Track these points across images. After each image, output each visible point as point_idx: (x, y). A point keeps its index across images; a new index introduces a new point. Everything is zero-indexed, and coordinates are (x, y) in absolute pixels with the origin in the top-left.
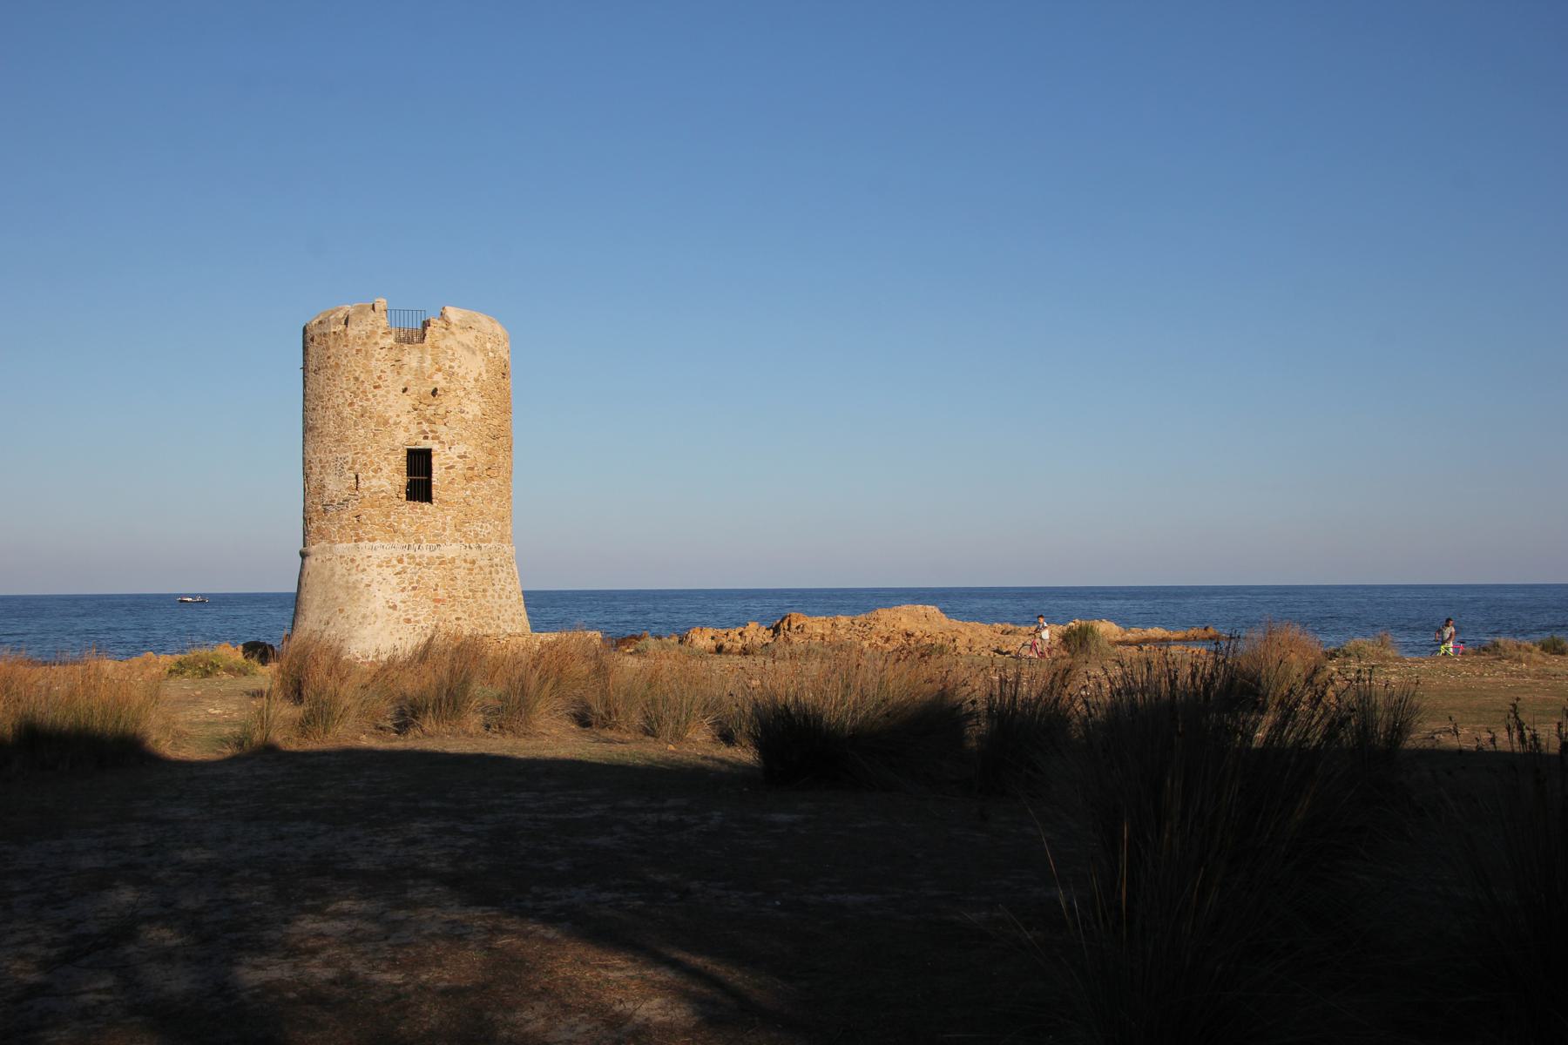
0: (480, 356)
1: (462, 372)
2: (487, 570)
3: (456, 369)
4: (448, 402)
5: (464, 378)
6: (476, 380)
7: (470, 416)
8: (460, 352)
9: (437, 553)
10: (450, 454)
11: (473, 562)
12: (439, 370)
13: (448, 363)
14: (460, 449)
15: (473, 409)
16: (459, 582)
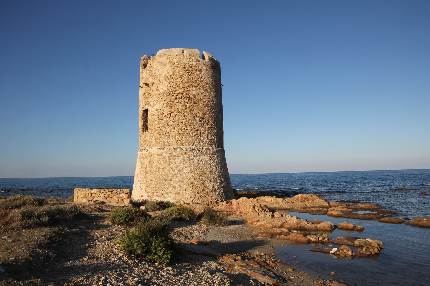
0: (168, 66)
1: (158, 74)
2: (168, 158)
3: (157, 74)
4: (153, 88)
5: (160, 76)
6: (165, 76)
7: (161, 92)
8: (158, 66)
9: (148, 152)
10: (153, 110)
11: (161, 155)
12: (151, 76)
13: (154, 72)
14: (157, 106)
15: (163, 88)
16: (154, 164)
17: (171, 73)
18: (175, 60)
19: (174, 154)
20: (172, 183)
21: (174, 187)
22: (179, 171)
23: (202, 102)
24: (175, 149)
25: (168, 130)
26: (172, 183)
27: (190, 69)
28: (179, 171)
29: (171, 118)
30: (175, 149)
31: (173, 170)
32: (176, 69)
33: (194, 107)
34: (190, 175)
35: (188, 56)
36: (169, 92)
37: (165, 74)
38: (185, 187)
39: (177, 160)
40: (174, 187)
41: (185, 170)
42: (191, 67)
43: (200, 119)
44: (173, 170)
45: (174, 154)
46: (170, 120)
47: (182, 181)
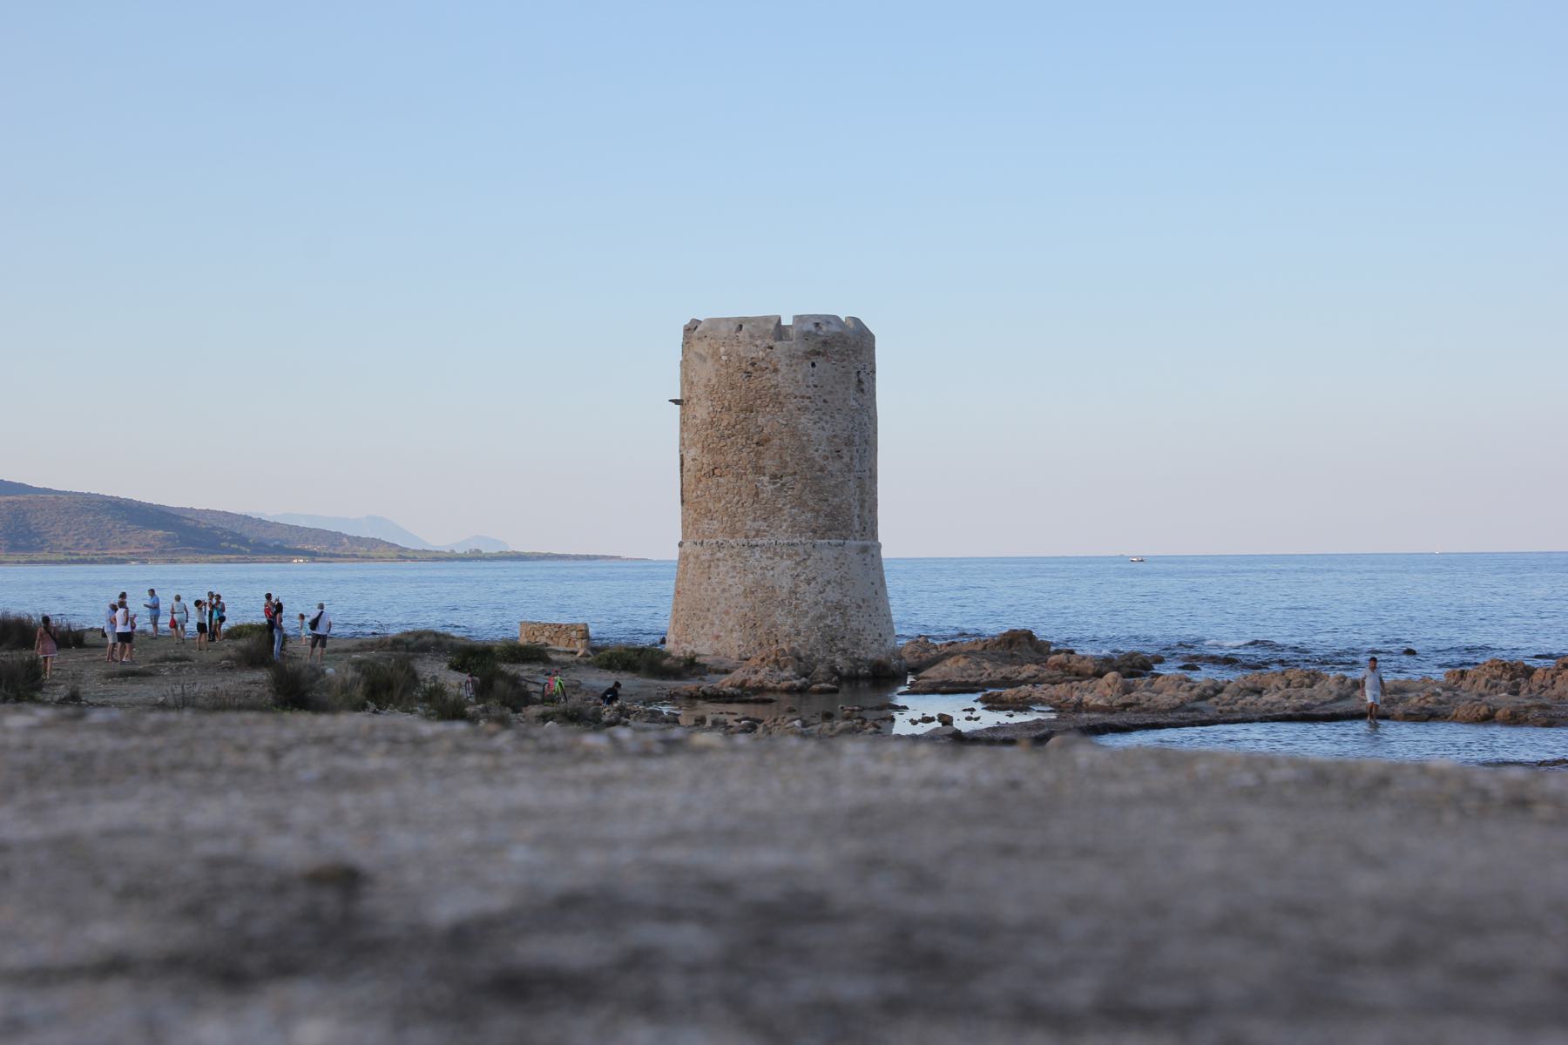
0: (710, 362)
17: (714, 381)
18: (722, 350)
19: (719, 555)
20: (710, 615)
21: (712, 624)
22: (724, 590)
23: (776, 441)
24: (720, 546)
25: (711, 505)
26: (710, 615)
27: (750, 369)
28: (724, 590)
29: (715, 480)
30: (720, 546)
31: (714, 590)
32: (723, 371)
33: (758, 454)
34: (741, 600)
35: (748, 340)
36: (712, 423)
37: (704, 381)
38: (730, 624)
39: (722, 569)
40: (712, 624)
41: (734, 591)
42: (753, 364)
43: (774, 476)
44: (714, 590)
45: (719, 555)
46: (712, 482)
47: (727, 613)
